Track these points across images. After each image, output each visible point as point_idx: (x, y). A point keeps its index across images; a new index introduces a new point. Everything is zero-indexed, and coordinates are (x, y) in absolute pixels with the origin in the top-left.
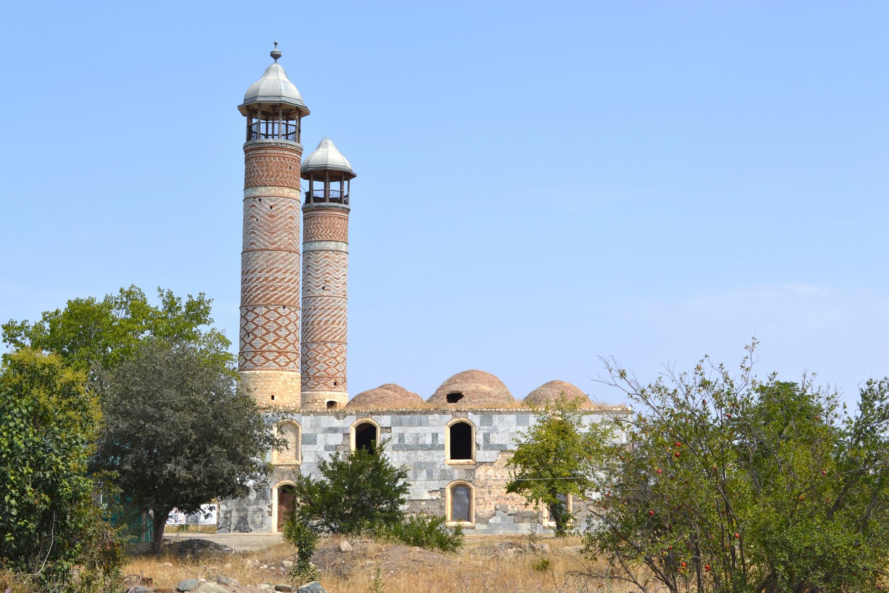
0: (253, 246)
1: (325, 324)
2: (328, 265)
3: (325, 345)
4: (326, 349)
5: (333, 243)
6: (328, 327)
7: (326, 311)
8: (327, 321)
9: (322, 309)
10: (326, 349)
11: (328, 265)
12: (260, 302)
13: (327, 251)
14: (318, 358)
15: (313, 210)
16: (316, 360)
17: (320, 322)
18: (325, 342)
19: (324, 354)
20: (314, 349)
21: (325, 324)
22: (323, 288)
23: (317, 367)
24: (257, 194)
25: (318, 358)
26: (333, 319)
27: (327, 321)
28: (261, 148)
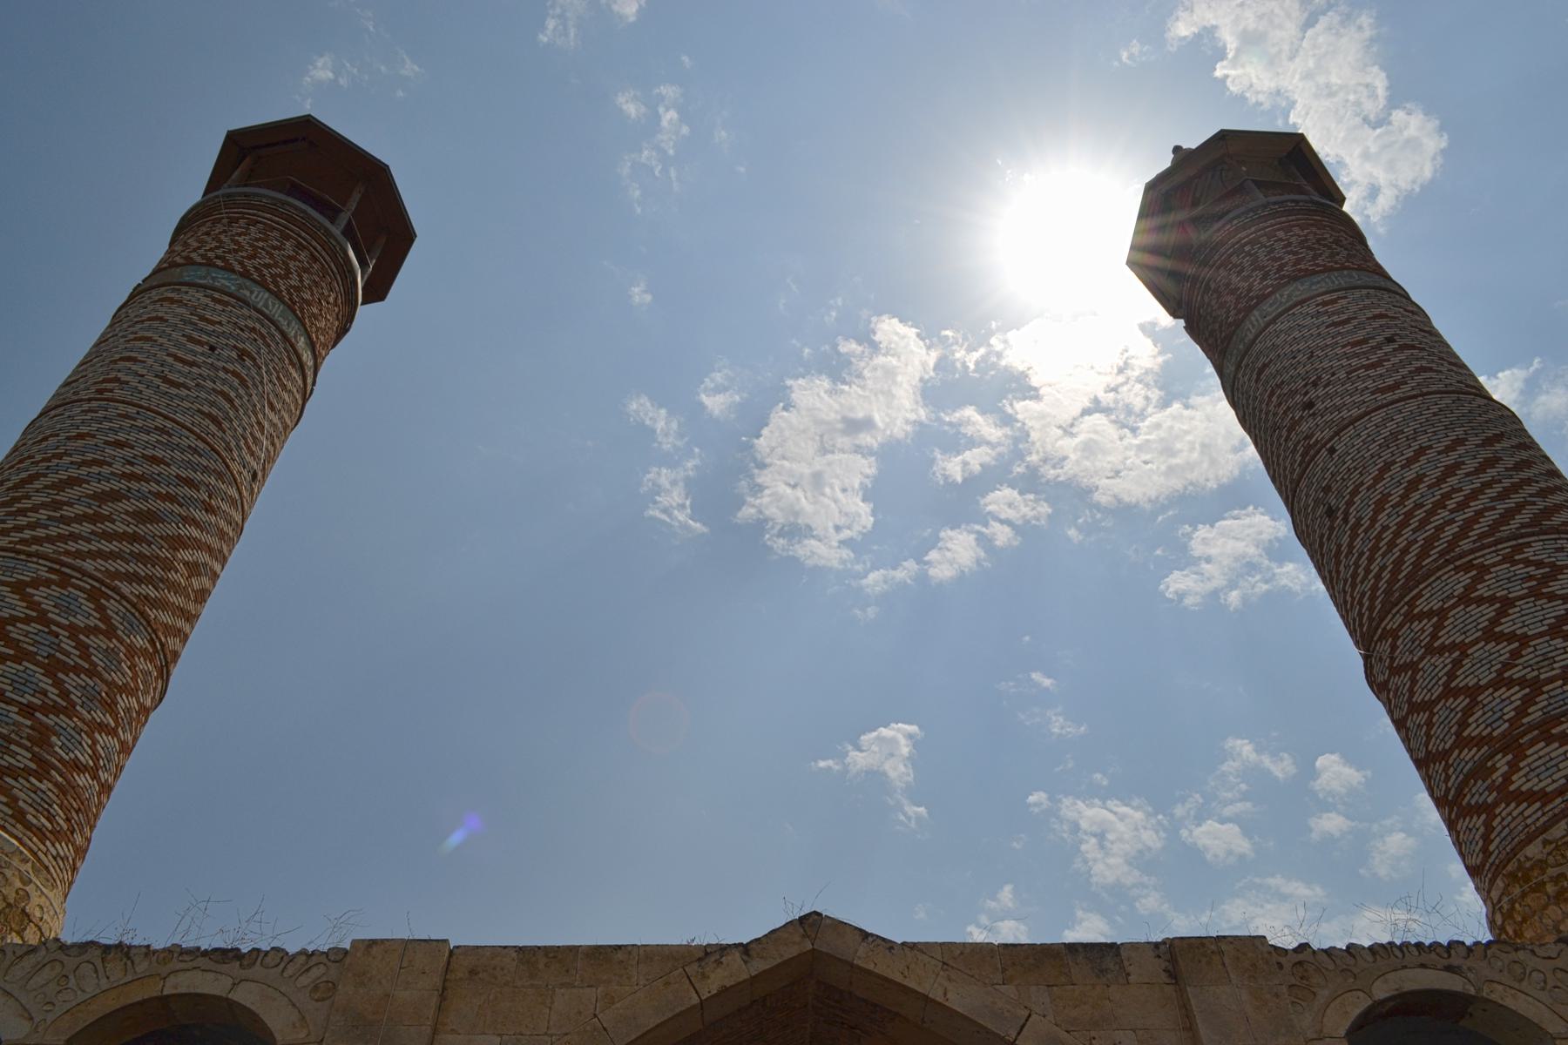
14: (123, 702)
16: (110, 707)
20: (132, 651)
25: (123, 702)
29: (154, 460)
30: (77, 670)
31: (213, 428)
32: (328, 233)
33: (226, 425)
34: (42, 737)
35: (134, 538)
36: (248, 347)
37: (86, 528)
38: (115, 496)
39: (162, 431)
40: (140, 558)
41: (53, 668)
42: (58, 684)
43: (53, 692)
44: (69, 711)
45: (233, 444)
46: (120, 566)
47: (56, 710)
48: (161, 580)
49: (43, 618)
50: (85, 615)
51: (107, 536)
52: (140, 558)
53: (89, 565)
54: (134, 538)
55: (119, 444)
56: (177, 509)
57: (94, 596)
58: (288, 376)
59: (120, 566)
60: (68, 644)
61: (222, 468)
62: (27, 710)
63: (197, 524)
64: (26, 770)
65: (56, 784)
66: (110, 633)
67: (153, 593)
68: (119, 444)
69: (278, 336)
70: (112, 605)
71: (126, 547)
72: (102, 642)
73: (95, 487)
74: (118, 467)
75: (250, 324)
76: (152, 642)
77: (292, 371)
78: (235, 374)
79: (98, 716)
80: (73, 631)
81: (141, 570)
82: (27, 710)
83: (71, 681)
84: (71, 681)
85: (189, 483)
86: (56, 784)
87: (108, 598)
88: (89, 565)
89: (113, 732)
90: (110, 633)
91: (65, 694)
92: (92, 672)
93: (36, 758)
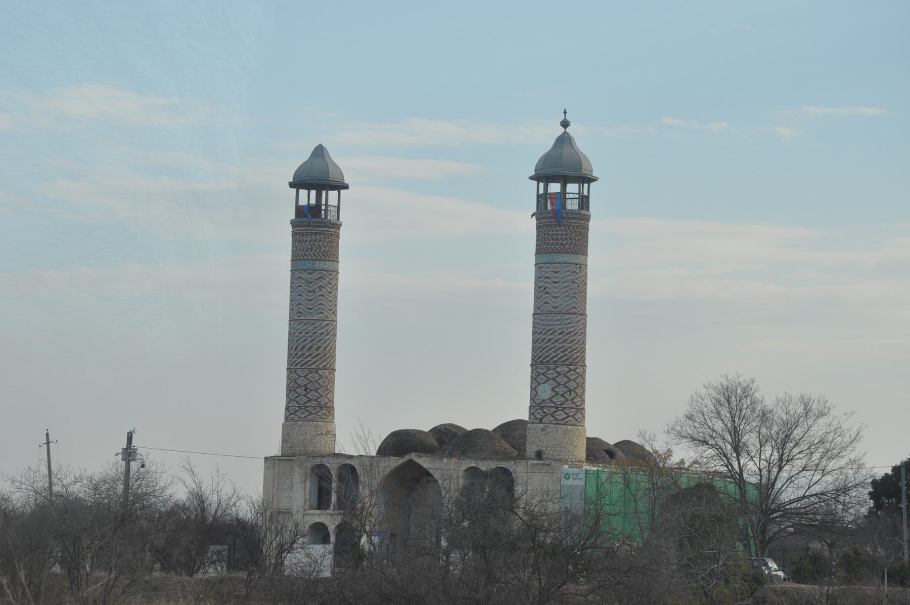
0: (574, 310)
24: (578, 261)
28: (581, 219)
29: (315, 333)
34: (319, 403)
37: (309, 358)
38: (311, 347)
39: (313, 324)
41: (316, 390)
44: (322, 396)
49: (311, 382)
51: (313, 358)
53: (313, 366)
55: (307, 333)
57: (316, 372)
68: (307, 333)
73: (307, 347)
74: (310, 339)
84: (319, 391)
85: (322, 333)
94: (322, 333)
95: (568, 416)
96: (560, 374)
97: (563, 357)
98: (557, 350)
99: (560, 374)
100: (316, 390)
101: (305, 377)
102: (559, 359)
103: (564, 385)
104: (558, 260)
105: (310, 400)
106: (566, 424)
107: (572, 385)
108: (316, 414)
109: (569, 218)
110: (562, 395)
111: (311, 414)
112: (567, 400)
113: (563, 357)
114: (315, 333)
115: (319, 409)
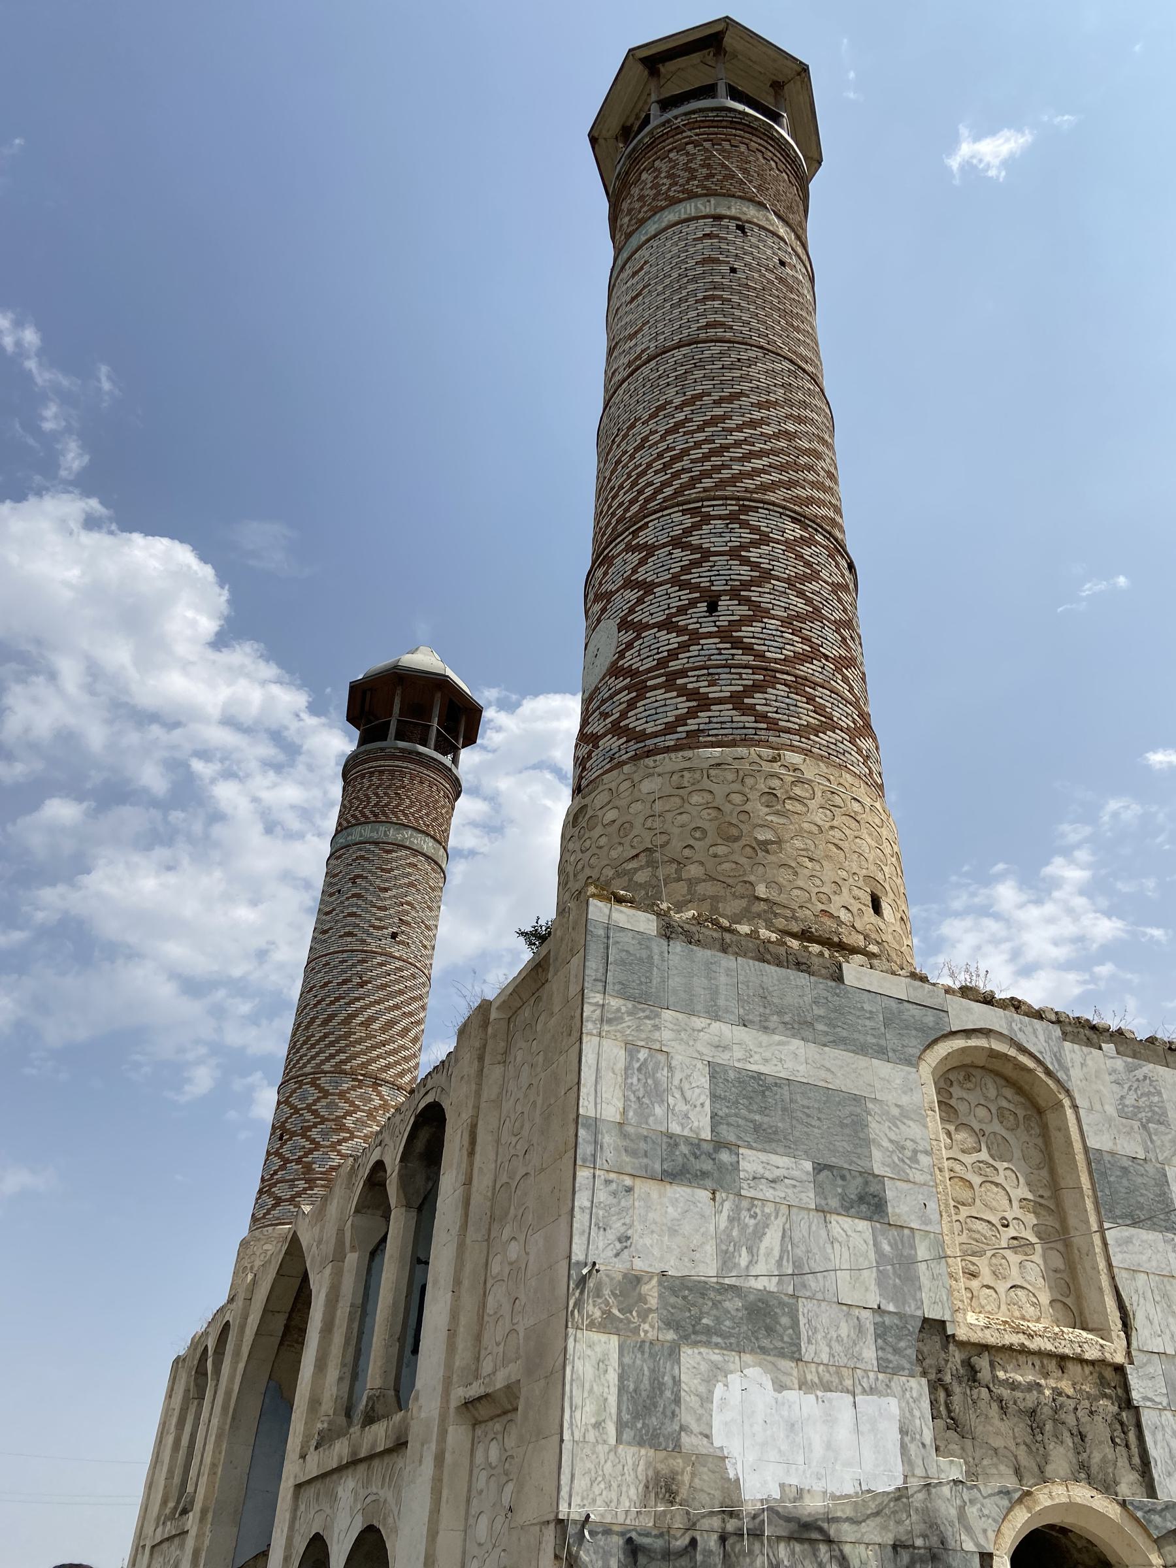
1: (383, 1030)
2: (411, 885)
3: (375, 1085)
4: (377, 1102)
5: (431, 842)
6: (391, 1040)
7: (392, 995)
8: (391, 1024)
9: (383, 987)
10: (377, 1102)
11: (411, 885)
12: (770, 497)
13: (417, 852)
14: (349, 1122)
15: (393, 757)
16: (342, 1128)
17: (372, 1019)
18: (377, 1083)
19: (370, 1115)
20: (342, 1095)
21: (383, 1030)
22: (394, 936)
23: (343, 1148)
26: (405, 1022)
27: (391, 1024)
29: (326, 984)
30: (315, 1125)
31: (349, 939)
32: (382, 749)
33: (356, 931)
34: (308, 1168)
35: (326, 1036)
36: (358, 872)
40: (332, 1044)
41: (304, 1133)
42: (308, 1138)
43: (307, 1145)
44: (317, 1146)
45: (364, 936)
46: (322, 1057)
47: (311, 1151)
48: (347, 1046)
50: (314, 1093)
51: (313, 1046)
52: (332, 1044)
53: (308, 1069)
54: (326, 1036)
56: (342, 1002)
57: (313, 1084)
58: (389, 861)
59: (322, 1057)
60: (308, 1116)
61: (361, 956)
62: (299, 1161)
63: (358, 999)
64: (305, 1189)
65: (322, 1186)
66: (326, 1094)
67: (343, 1056)
69: (372, 847)
70: (323, 1081)
71: (322, 1045)
72: (324, 1102)
75: (354, 857)
76: (354, 1080)
77: (394, 855)
78: (354, 896)
79: (335, 1138)
80: (308, 1108)
81: (332, 1050)
82: (299, 1161)
83: (314, 1133)
84: (314, 1133)
85: (345, 982)
86: (322, 1186)
87: (319, 1079)
88: (308, 1069)
89: (352, 1137)
90: (326, 1094)
91: (313, 1141)
92: (324, 1120)
93: (307, 1181)
94: (345, 982)
95: (705, 703)
96: (650, 550)
97: (665, 484)
98: (643, 473)
99: (650, 550)
100: (304, 1133)
101: (287, 1102)
102: (648, 500)
103: (675, 581)
104: (644, 238)
105: (287, 1161)
106: (693, 740)
107: (722, 573)
108: (291, 1200)
109: (678, 130)
110: (667, 625)
111: (278, 1201)
112: (695, 637)
113: (665, 484)
114: (326, 984)
115: (302, 1184)
